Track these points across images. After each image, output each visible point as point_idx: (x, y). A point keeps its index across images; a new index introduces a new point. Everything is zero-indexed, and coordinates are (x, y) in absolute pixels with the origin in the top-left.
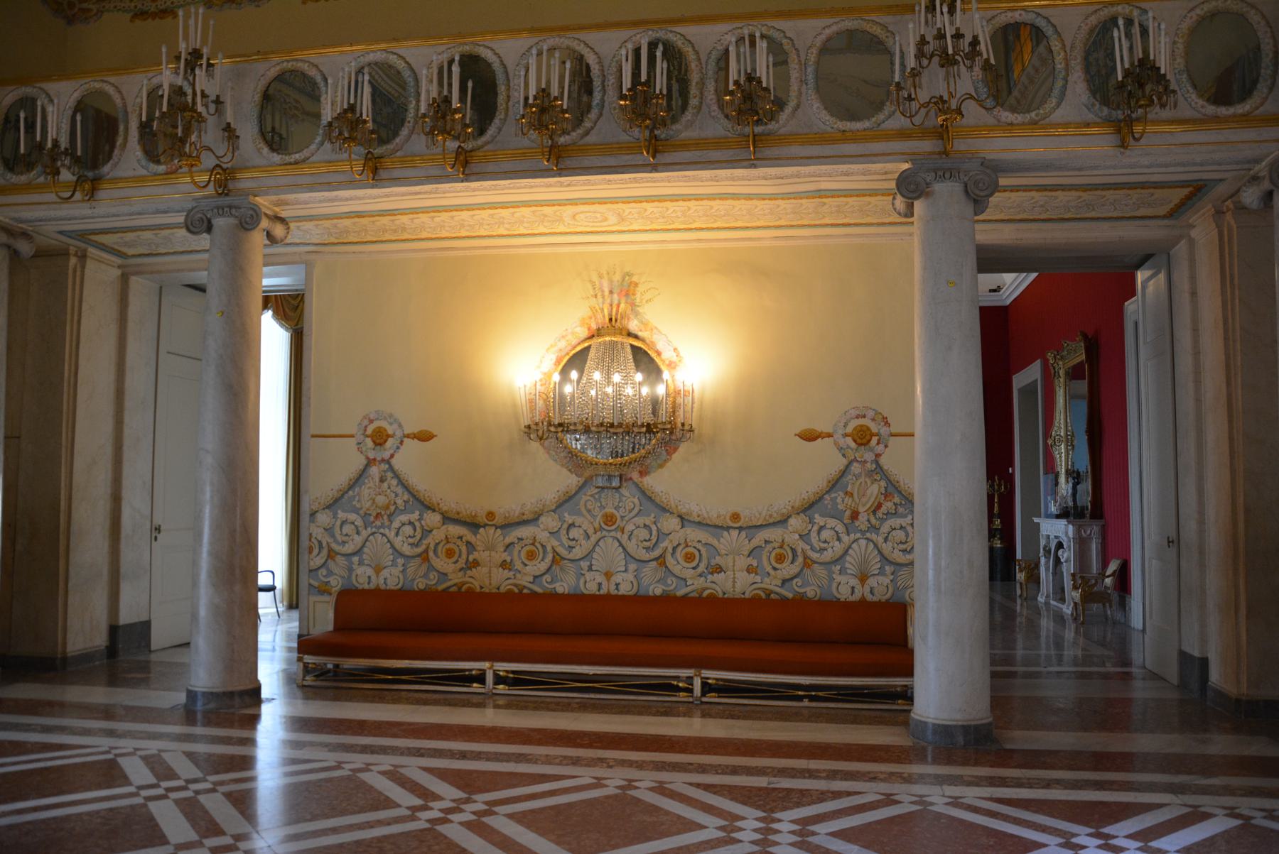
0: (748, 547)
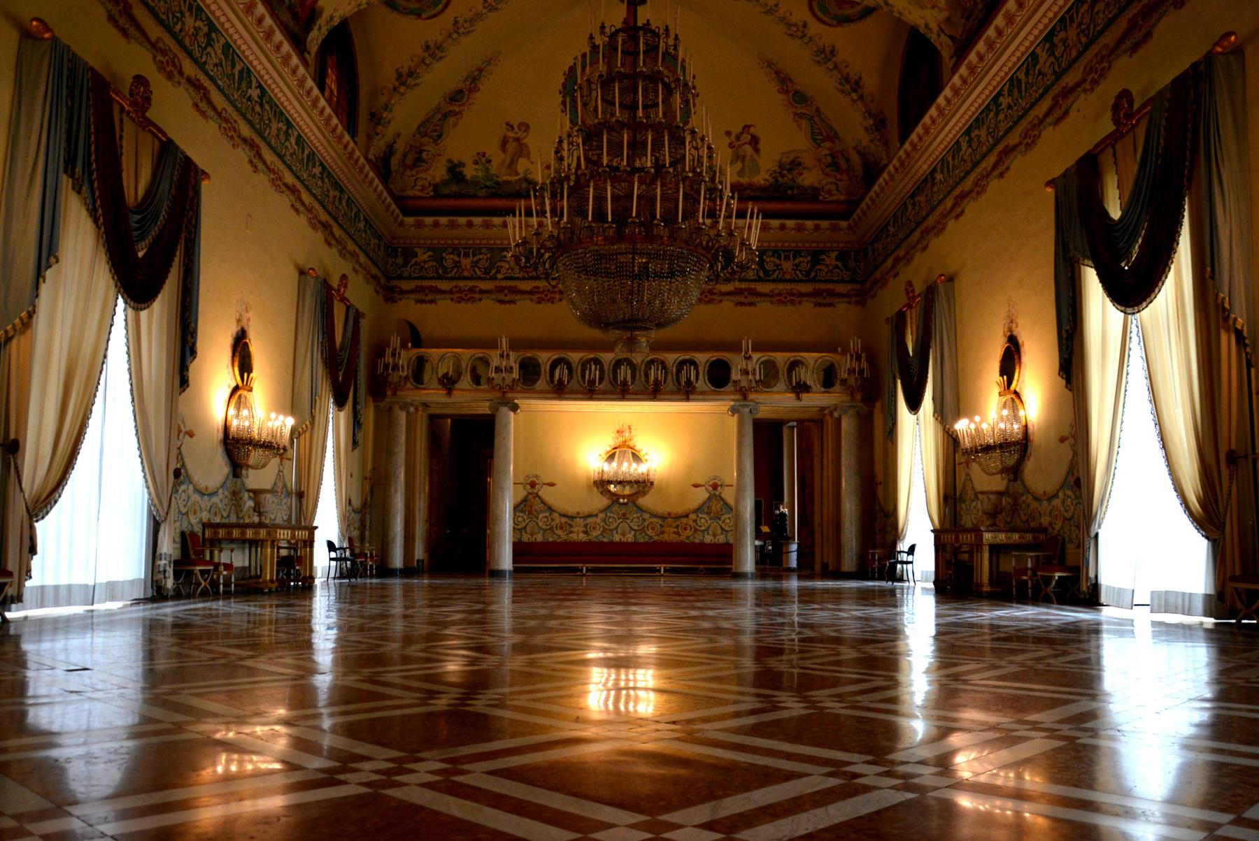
0: (674, 525)
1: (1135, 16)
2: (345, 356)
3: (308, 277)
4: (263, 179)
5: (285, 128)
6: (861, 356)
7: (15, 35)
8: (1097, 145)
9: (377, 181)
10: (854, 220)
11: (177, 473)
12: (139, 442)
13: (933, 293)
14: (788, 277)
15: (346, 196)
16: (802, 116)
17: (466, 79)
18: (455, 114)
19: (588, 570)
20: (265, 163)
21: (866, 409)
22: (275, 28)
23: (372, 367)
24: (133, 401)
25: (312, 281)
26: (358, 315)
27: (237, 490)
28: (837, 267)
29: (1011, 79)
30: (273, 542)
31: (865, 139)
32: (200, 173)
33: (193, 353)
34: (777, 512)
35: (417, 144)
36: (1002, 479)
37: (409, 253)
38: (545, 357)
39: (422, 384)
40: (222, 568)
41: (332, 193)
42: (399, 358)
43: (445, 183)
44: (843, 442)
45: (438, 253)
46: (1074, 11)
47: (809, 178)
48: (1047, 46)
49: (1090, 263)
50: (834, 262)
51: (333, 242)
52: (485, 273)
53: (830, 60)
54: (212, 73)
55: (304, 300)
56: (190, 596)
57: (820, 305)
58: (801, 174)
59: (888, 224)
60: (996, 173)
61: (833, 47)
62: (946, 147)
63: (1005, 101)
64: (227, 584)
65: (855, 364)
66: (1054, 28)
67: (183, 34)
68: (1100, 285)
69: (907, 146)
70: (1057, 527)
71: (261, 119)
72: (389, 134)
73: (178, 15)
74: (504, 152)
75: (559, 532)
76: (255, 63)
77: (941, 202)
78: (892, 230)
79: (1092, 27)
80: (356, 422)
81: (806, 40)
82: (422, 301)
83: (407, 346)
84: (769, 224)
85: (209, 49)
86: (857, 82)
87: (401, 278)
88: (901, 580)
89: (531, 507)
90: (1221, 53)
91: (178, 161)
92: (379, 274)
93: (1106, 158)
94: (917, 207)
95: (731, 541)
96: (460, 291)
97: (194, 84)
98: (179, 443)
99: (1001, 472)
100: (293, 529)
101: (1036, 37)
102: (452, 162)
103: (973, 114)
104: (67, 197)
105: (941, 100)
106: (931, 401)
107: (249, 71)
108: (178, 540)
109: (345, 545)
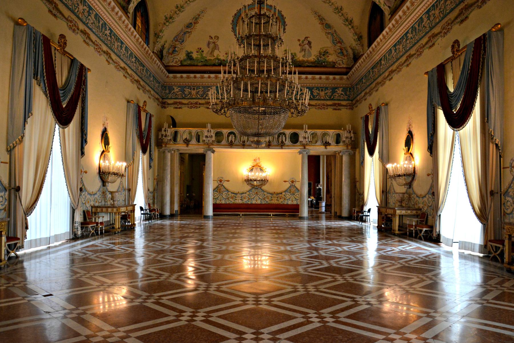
0: (276, 197)
1: (462, 9)
2: (146, 133)
3: (131, 104)
4: (112, 66)
5: (120, 45)
6: (351, 132)
7: (12, 24)
8: (445, 61)
9: (158, 61)
10: (349, 76)
11: (81, 190)
12: (66, 180)
13: (379, 110)
14: (322, 98)
15: (145, 68)
16: (329, 33)
17: (193, 19)
18: (189, 32)
19: (242, 215)
20: (113, 60)
21: (353, 152)
22: (116, 6)
23: (157, 136)
24: (63, 164)
25: (132, 105)
26: (151, 116)
27: (104, 191)
28: (342, 94)
29: (412, 27)
30: (119, 213)
31: (354, 44)
32: (87, 69)
33: (86, 142)
34: (318, 188)
35: (174, 44)
36: (405, 187)
37: (171, 89)
38: (225, 131)
39: (177, 142)
40: (99, 225)
41: (140, 68)
42: (167, 132)
43: (185, 60)
44: (343, 165)
45: (182, 88)
46: (438, 3)
47: (331, 58)
48: (427, 15)
49: (441, 108)
50: (341, 92)
51: (140, 87)
52: (201, 97)
53: (340, 12)
54: (90, 27)
55: (129, 111)
56: (87, 237)
57: (335, 109)
58: (328, 57)
59: (362, 78)
60: (406, 64)
61: (342, 7)
62: (386, 51)
63: (410, 35)
64: (101, 231)
65: (349, 135)
66: (430, 9)
67: (78, 13)
68: (445, 117)
69: (370, 49)
70: (426, 208)
71: (111, 42)
72: (162, 41)
73: (76, 5)
74: (209, 48)
75: (231, 200)
76: (108, 20)
77: (383, 73)
78: (364, 81)
79: (445, 10)
80: (151, 158)
81: (330, 4)
82: (176, 108)
83: (170, 127)
84: (315, 77)
85: (89, 17)
86: (351, 21)
87: (167, 98)
88: (365, 221)
89: (220, 190)
90: (495, 31)
91: (78, 66)
92: (159, 97)
93: (448, 67)
94: (374, 73)
95: (299, 204)
96: (191, 104)
97: (84, 32)
98: (81, 176)
99: (405, 185)
100: (127, 207)
101: (423, 12)
102: (188, 52)
103: (397, 39)
104: (35, 87)
105: (384, 32)
106: (378, 153)
107: (105, 24)
108: (82, 214)
109: (147, 207)
